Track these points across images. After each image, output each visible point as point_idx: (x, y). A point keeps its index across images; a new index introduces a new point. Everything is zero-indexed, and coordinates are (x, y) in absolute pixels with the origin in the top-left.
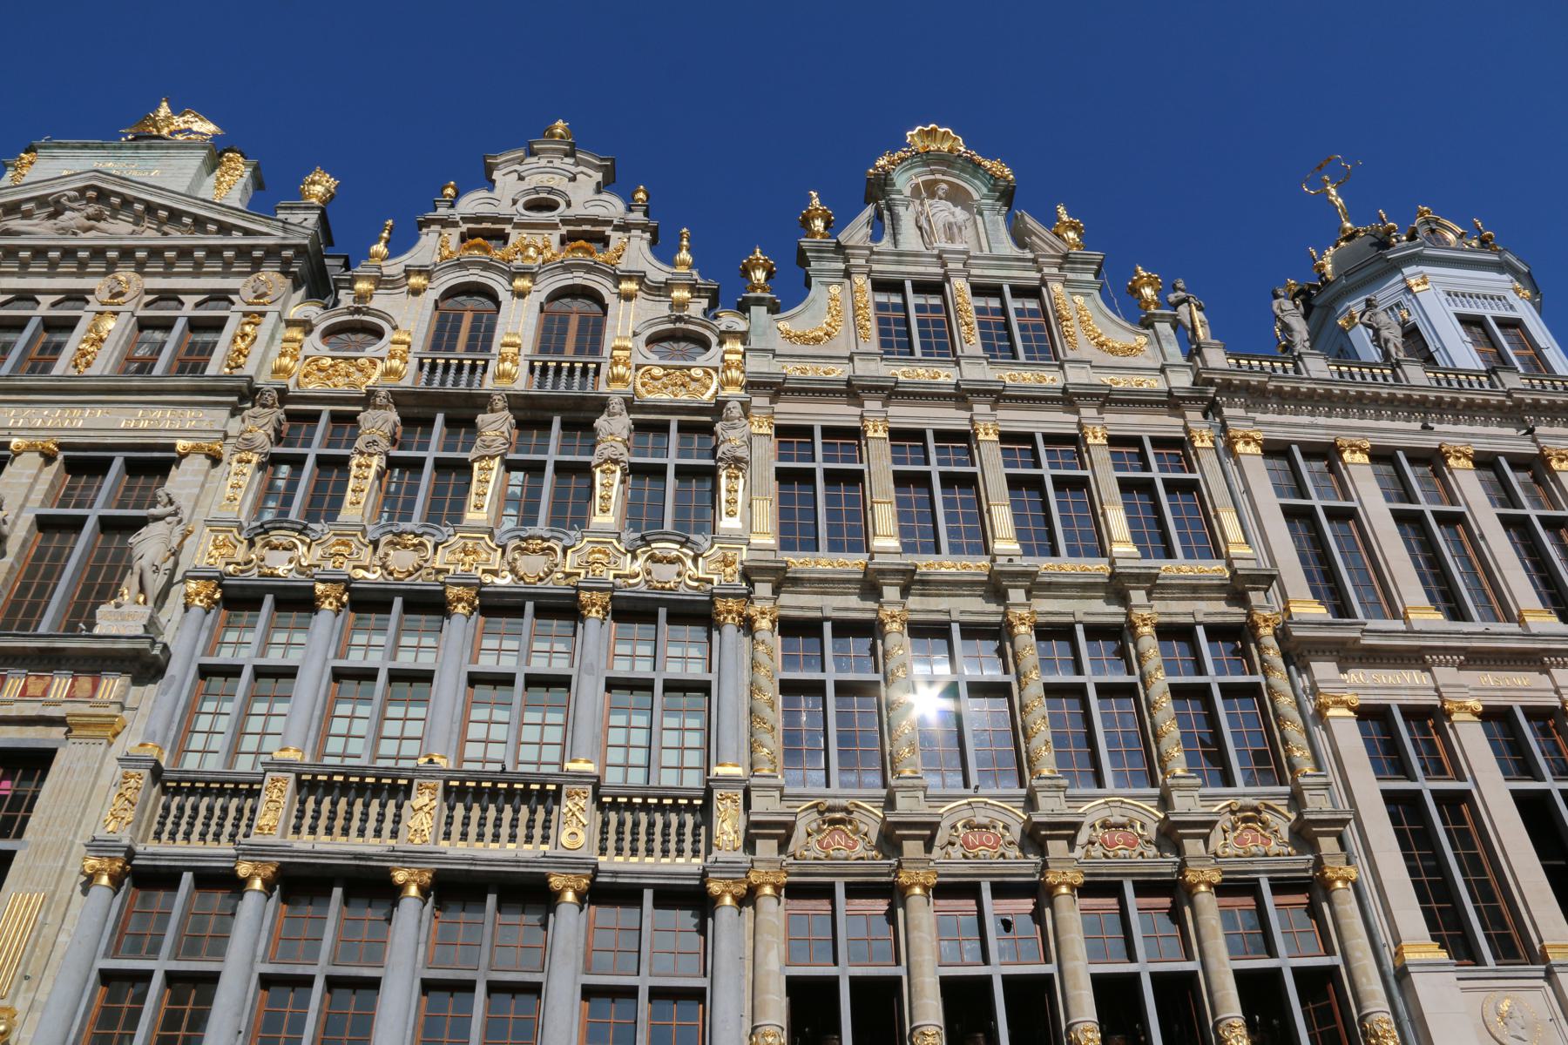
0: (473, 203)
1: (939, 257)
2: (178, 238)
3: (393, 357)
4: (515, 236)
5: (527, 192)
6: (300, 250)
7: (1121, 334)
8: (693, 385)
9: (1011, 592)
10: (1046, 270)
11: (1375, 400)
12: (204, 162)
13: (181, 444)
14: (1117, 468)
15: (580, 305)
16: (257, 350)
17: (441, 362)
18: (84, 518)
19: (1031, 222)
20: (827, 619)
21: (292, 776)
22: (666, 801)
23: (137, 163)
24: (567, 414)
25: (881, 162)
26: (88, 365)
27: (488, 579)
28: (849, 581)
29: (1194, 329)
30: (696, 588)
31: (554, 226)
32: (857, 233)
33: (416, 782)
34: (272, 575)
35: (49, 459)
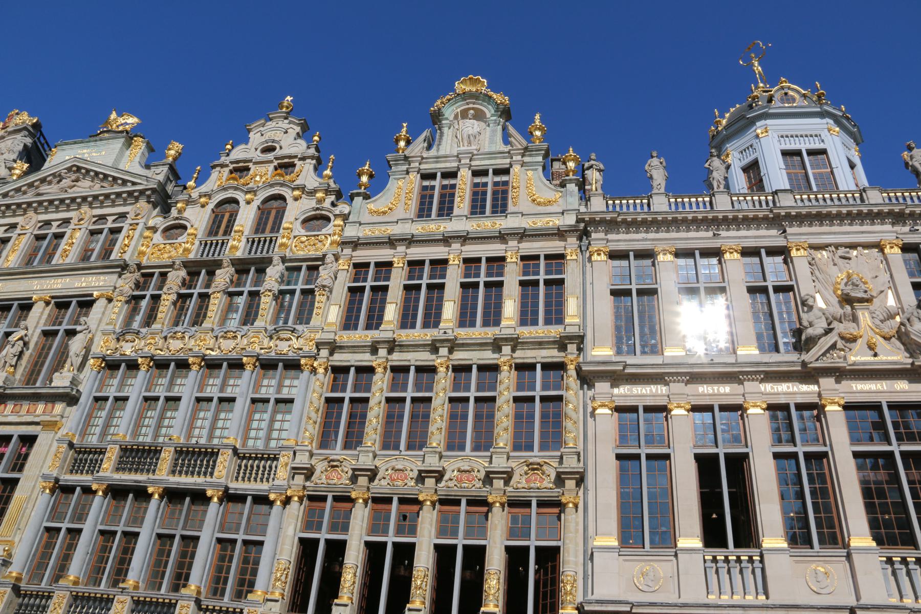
0: (239, 153)
1: (457, 156)
5: (263, 143)
6: (154, 190)
7: (546, 192)
8: (319, 245)
11: (685, 220)
12: (124, 144)
13: (95, 294)
15: (275, 204)
18: (58, 330)
19: (511, 130)
21: (118, 446)
24: (258, 266)
25: (439, 102)
28: (365, 346)
31: (271, 162)
32: (418, 147)
35: (47, 303)
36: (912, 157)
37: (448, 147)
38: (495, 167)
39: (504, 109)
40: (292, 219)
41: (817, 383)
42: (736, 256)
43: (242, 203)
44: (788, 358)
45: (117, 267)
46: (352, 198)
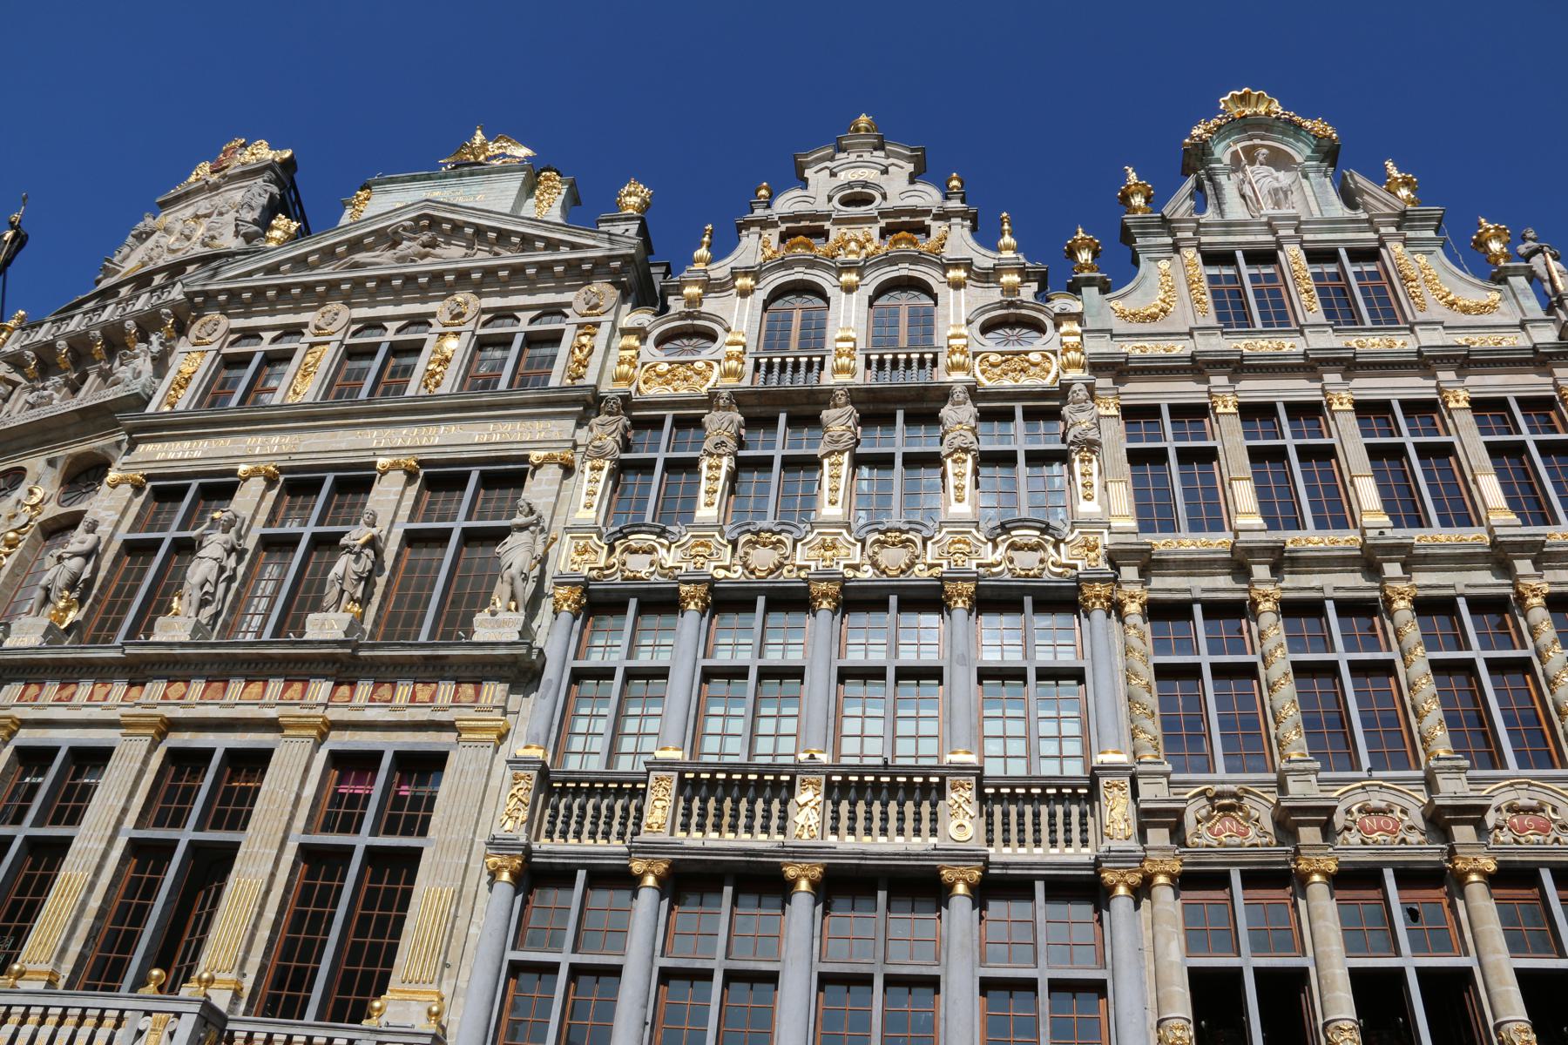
0: (788, 203)
1: (1269, 224)
2: (509, 257)
3: (729, 358)
4: (835, 233)
5: (842, 187)
7: (1473, 292)
8: (1032, 370)
9: (1386, 566)
10: (1383, 230)
12: (524, 183)
14: (1483, 432)
16: (595, 361)
17: (803, 360)
19: (1362, 181)
20: (1196, 601)
22: (1049, 791)
23: (462, 189)
24: (910, 406)
25: (1195, 132)
26: (437, 385)
27: (850, 573)
29: (1552, 281)
30: (1060, 575)
31: (873, 220)
32: (1180, 206)
33: (798, 778)
34: (635, 578)
38: (1349, 245)
45: (575, 402)
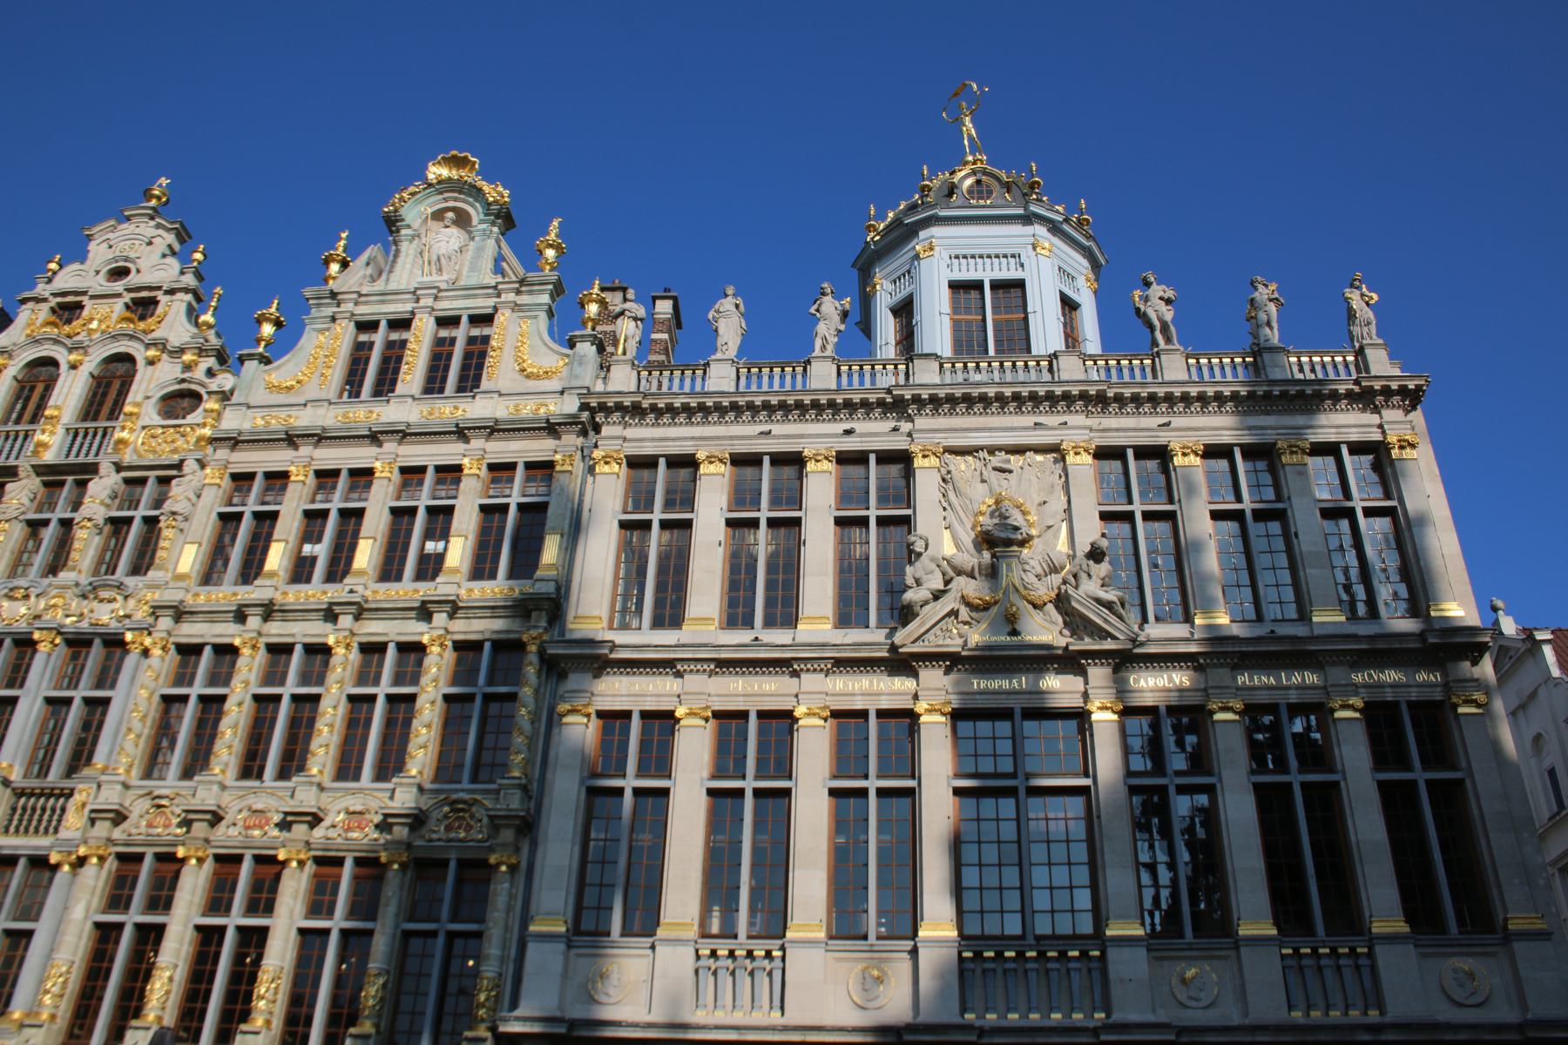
1: (414, 293)
5: (109, 262)
7: (548, 357)
15: (121, 368)
31: (119, 295)
36: (1146, 299)
37: (405, 276)
39: (500, 211)
40: (139, 398)
41: (916, 675)
42: (827, 466)
43: (64, 367)
44: (871, 637)
46: (241, 360)
